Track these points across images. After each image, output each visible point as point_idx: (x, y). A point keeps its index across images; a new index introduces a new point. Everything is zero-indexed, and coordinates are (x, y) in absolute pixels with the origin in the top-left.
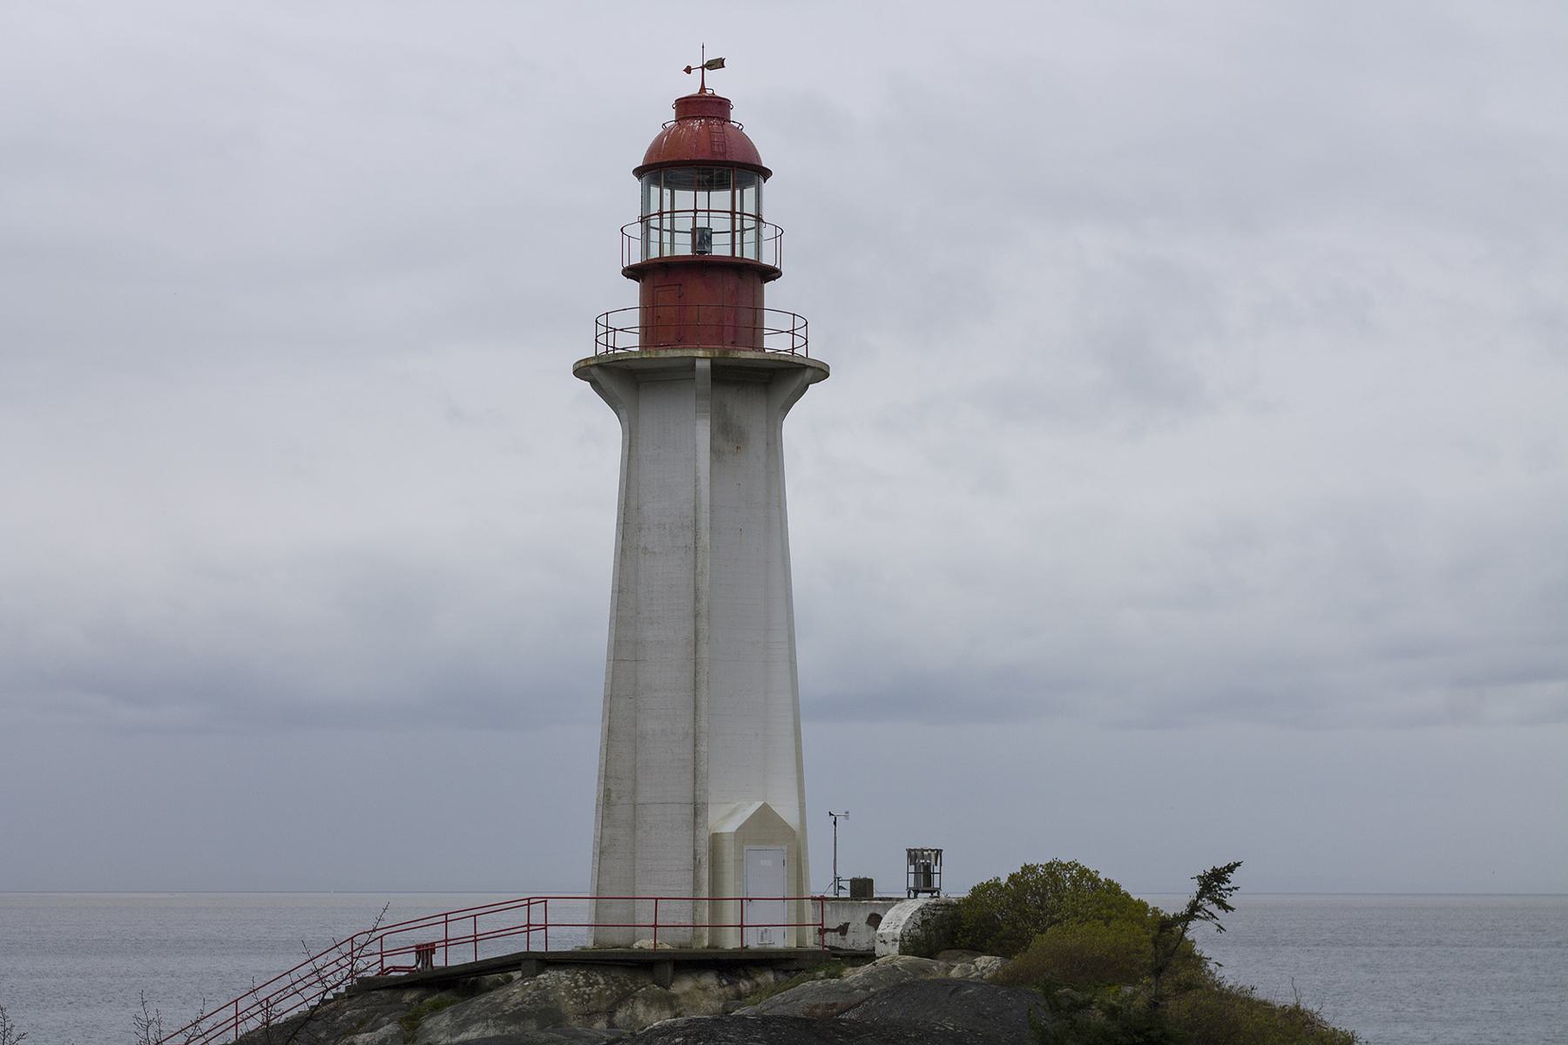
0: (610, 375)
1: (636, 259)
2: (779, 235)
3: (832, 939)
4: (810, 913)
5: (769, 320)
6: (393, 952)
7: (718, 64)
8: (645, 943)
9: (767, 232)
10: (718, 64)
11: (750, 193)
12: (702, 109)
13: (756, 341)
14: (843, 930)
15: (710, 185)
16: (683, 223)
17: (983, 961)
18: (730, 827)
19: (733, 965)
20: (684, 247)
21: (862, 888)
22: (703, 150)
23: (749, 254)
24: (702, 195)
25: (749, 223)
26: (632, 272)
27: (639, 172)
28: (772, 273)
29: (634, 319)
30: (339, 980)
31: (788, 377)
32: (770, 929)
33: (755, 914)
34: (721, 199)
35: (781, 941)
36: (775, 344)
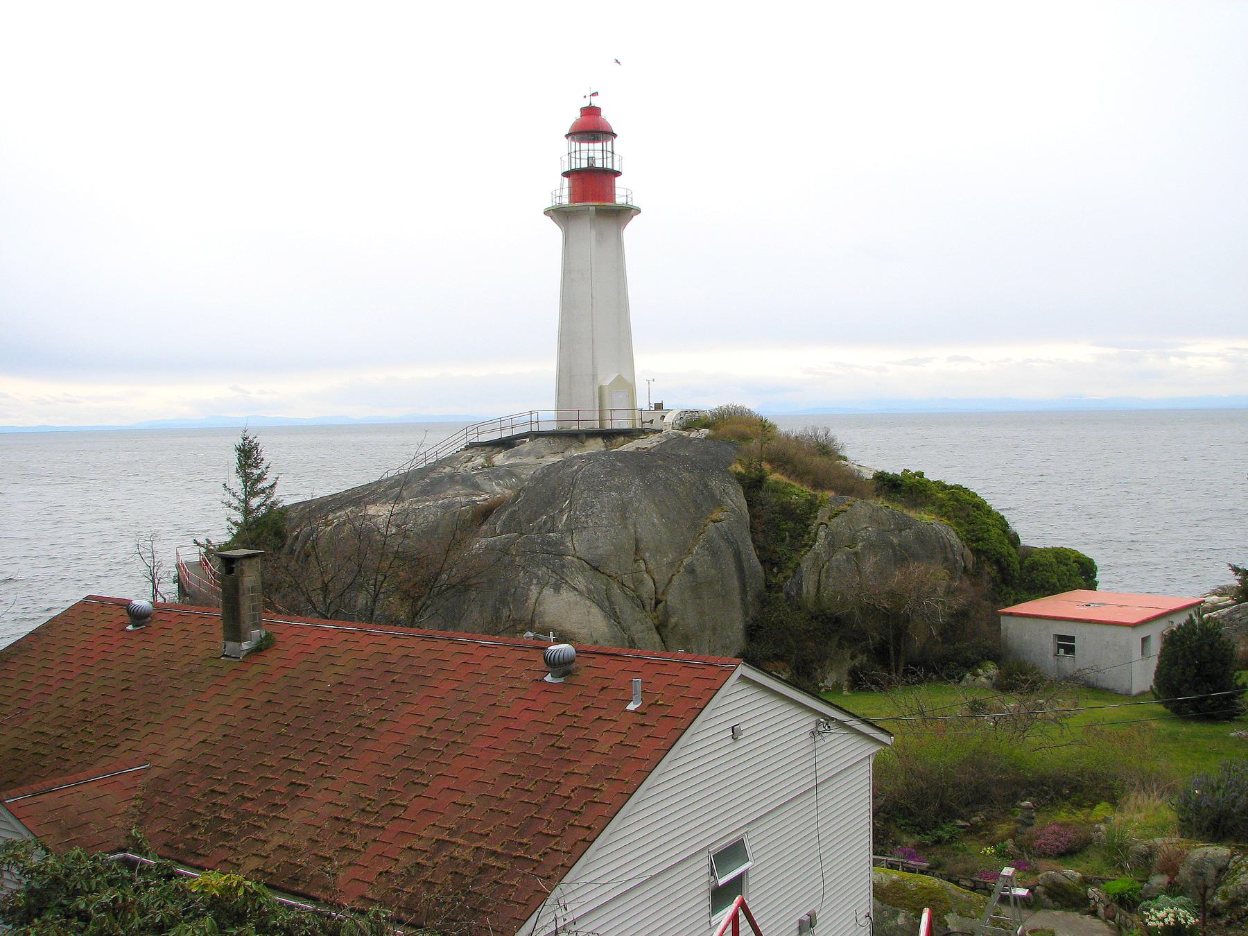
0: (559, 214)
1: (567, 169)
2: (621, 159)
3: (647, 425)
4: (638, 415)
5: (618, 191)
6: (483, 433)
7: (595, 94)
8: (575, 427)
9: (616, 158)
10: (595, 94)
11: (609, 143)
12: (591, 112)
13: (612, 199)
14: (651, 422)
15: (595, 140)
16: (584, 155)
17: (702, 431)
18: (607, 383)
19: (609, 435)
20: (584, 165)
21: (659, 407)
22: (591, 127)
23: (610, 167)
24: (591, 145)
25: (609, 155)
26: (566, 174)
27: (567, 136)
28: (618, 174)
29: (566, 192)
30: (463, 443)
31: (624, 213)
32: (620, 422)
33: (616, 415)
34: (598, 146)
35: (626, 425)
36: (620, 200)
